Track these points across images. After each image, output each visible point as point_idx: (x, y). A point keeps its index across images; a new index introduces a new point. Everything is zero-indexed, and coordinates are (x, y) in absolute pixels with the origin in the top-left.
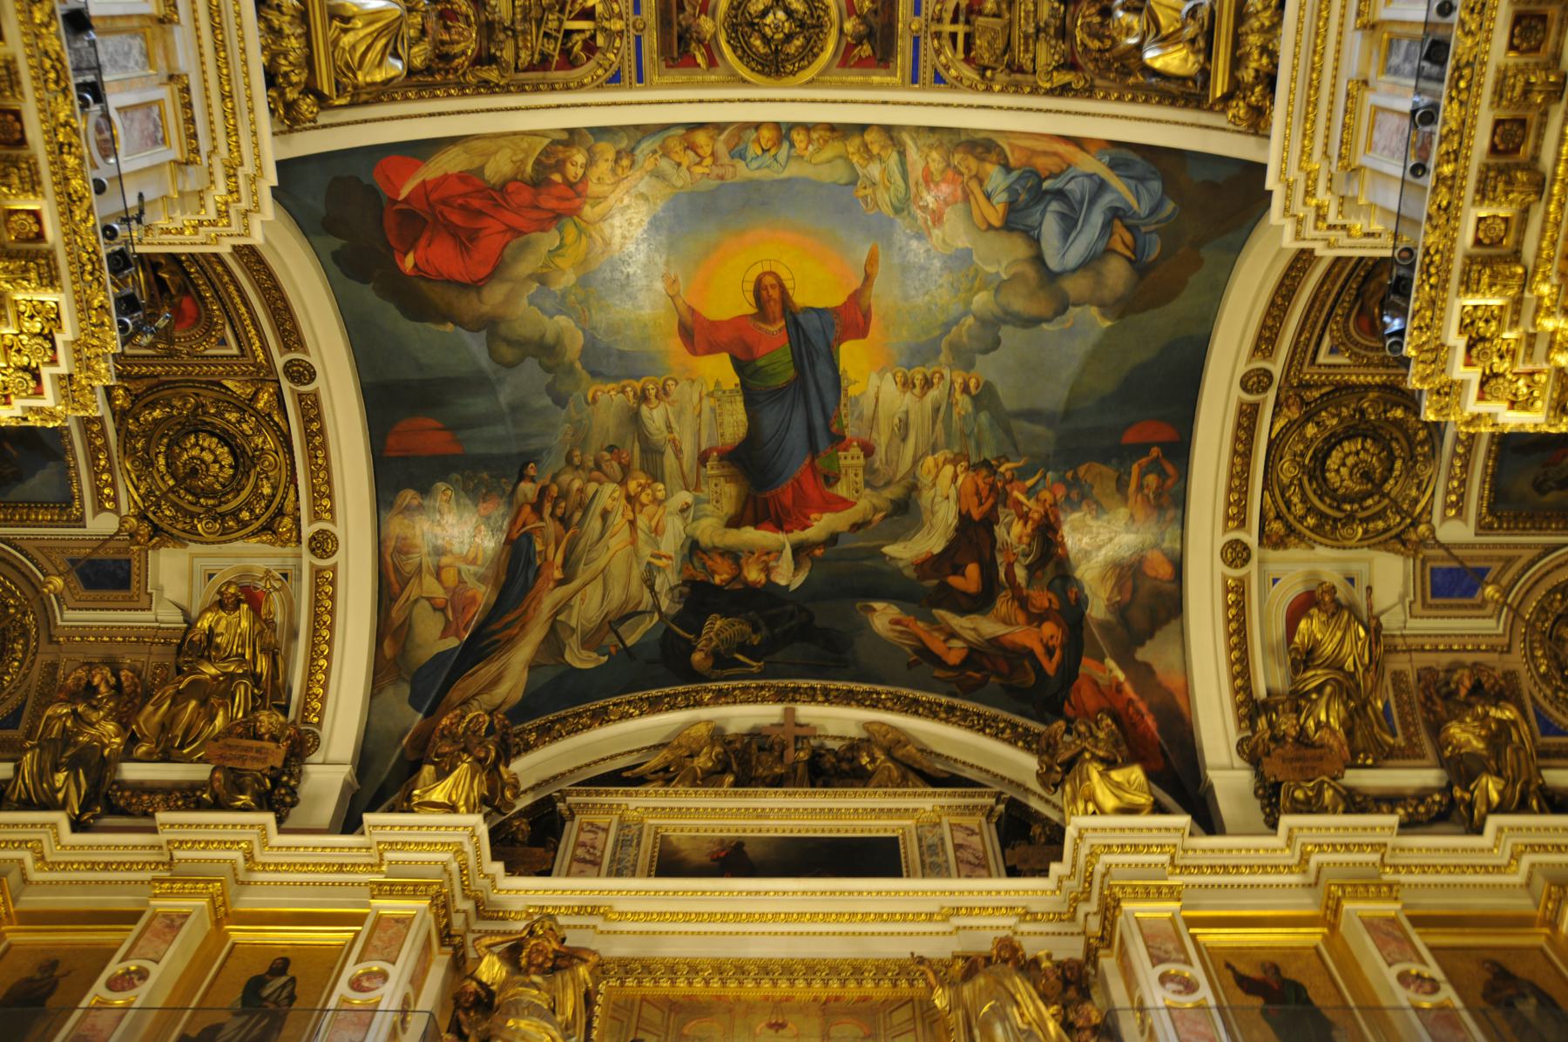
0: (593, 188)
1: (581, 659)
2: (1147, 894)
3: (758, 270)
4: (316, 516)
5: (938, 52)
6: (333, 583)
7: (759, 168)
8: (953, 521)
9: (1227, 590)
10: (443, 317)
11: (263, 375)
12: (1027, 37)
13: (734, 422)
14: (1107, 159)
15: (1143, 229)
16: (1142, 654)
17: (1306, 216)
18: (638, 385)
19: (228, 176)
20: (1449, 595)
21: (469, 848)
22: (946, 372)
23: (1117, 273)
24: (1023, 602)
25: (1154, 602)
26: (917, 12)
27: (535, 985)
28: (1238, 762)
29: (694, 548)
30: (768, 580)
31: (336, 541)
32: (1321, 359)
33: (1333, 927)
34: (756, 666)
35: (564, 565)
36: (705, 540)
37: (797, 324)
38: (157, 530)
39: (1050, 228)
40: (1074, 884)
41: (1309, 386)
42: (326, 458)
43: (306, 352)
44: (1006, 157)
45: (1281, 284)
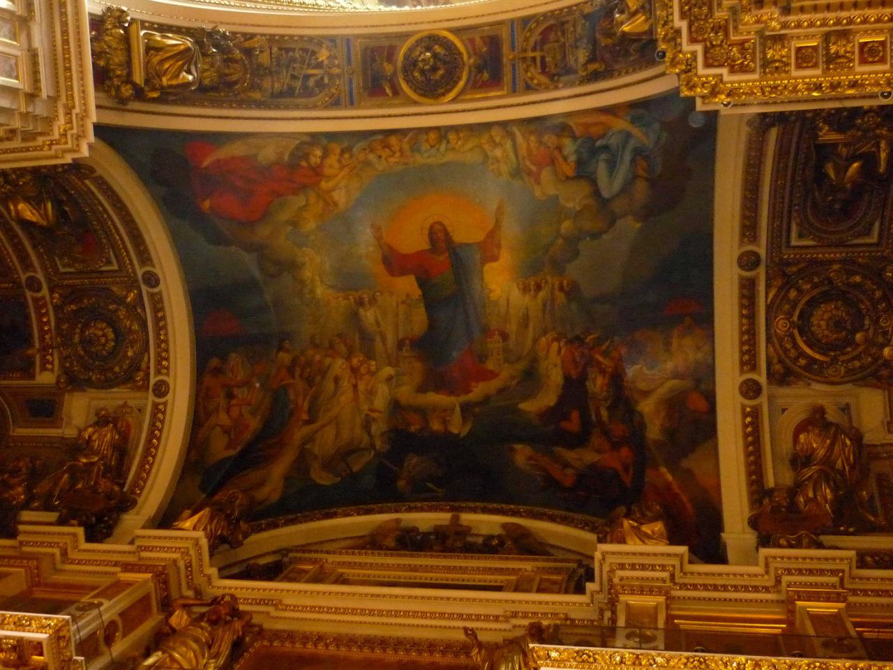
0: (327, 171)
1: (324, 479)
3: (430, 221)
4: (158, 372)
5: (526, 71)
6: (164, 413)
7: (428, 157)
9: (745, 415)
10: (228, 243)
11: (132, 284)
13: (419, 321)
14: (629, 118)
18: (357, 295)
19: (67, 114)
21: (192, 552)
22: (549, 278)
23: (641, 189)
24: (606, 433)
25: (693, 424)
26: (513, 48)
27: (202, 628)
29: (396, 406)
30: (446, 429)
31: (168, 386)
32: (794, 243)
34: (440, 492)
35: (309, 411)
36: (404, 401)
37: (456, 254)
38: (73, 382)
39: (602, 171)
41: (788, 264)
42: (166, 335)
43: (153, 266)
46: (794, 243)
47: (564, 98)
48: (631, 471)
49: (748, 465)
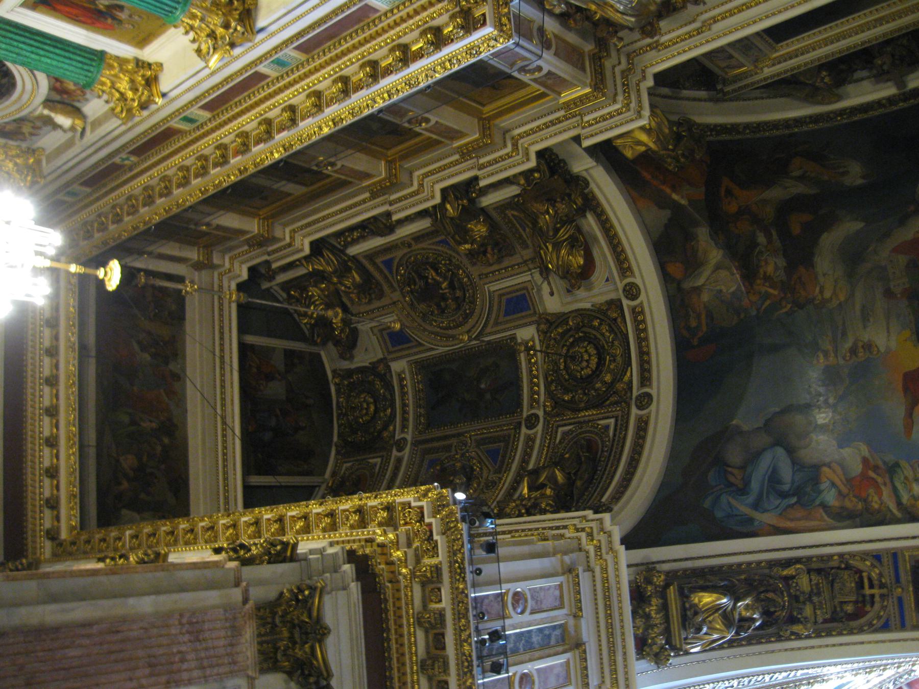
2: (581, 100)
8: (817, 260)
12: (819, 594)
14: (756, 523)
15: (722, 486)
17: (598, 534)
20: (517, 297)
22: (842, 362)
23: (734, 455)
25: (670, 247)
26: (900, 600)
28: (585, 174)
32: (612, 421)
33: (480, 119)
40: (633, 80)
41: (616, 403)
44: (826, 512)
45: (635, 468)
46: (612, 421)
47: (831, 545)
48: (723, 193)
49: (612, 226)
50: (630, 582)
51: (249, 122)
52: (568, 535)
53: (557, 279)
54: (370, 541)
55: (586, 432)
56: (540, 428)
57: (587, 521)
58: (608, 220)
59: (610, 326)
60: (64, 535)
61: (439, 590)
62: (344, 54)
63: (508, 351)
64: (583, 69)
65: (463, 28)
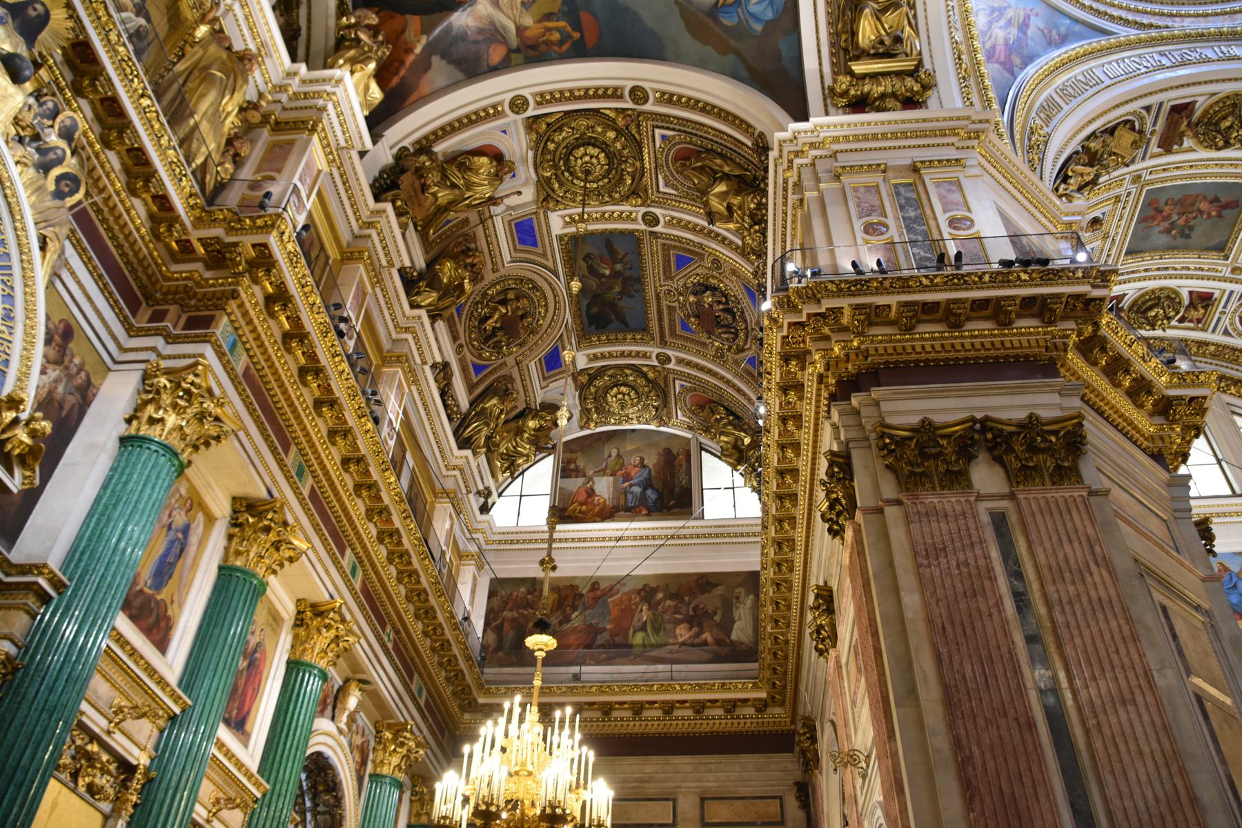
9: (494, 107)
16: (436, 60)
32: (657, 131)
46: (657, 131)
50: (845, 113)
51: (357, 508)
52: (796, 179)
53: (501, 187)
54: (821, 378)
55: (667, 161)
56: (658, 212)
57: (781, 156)
58: (442, 128)
59: (555, 131)
60: (763, 695)
61: (877, 307)
62: (291, 405)
63: (573, 244)
64: (291, 143)
65: (268, 271)
